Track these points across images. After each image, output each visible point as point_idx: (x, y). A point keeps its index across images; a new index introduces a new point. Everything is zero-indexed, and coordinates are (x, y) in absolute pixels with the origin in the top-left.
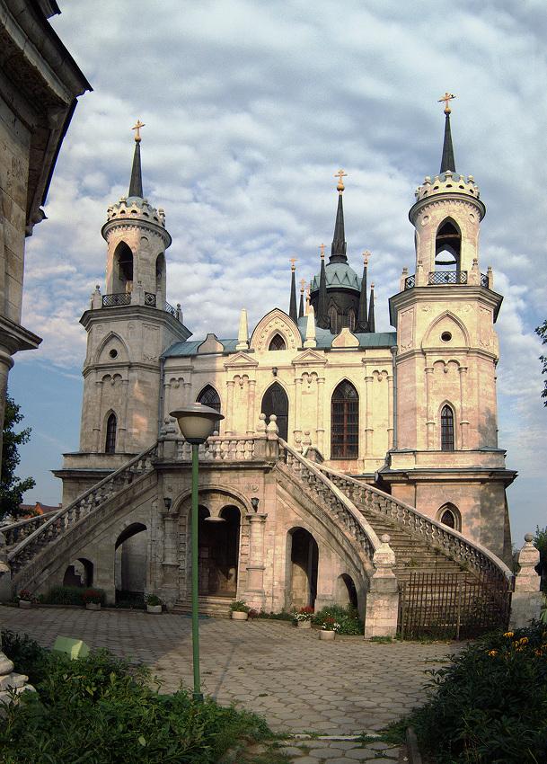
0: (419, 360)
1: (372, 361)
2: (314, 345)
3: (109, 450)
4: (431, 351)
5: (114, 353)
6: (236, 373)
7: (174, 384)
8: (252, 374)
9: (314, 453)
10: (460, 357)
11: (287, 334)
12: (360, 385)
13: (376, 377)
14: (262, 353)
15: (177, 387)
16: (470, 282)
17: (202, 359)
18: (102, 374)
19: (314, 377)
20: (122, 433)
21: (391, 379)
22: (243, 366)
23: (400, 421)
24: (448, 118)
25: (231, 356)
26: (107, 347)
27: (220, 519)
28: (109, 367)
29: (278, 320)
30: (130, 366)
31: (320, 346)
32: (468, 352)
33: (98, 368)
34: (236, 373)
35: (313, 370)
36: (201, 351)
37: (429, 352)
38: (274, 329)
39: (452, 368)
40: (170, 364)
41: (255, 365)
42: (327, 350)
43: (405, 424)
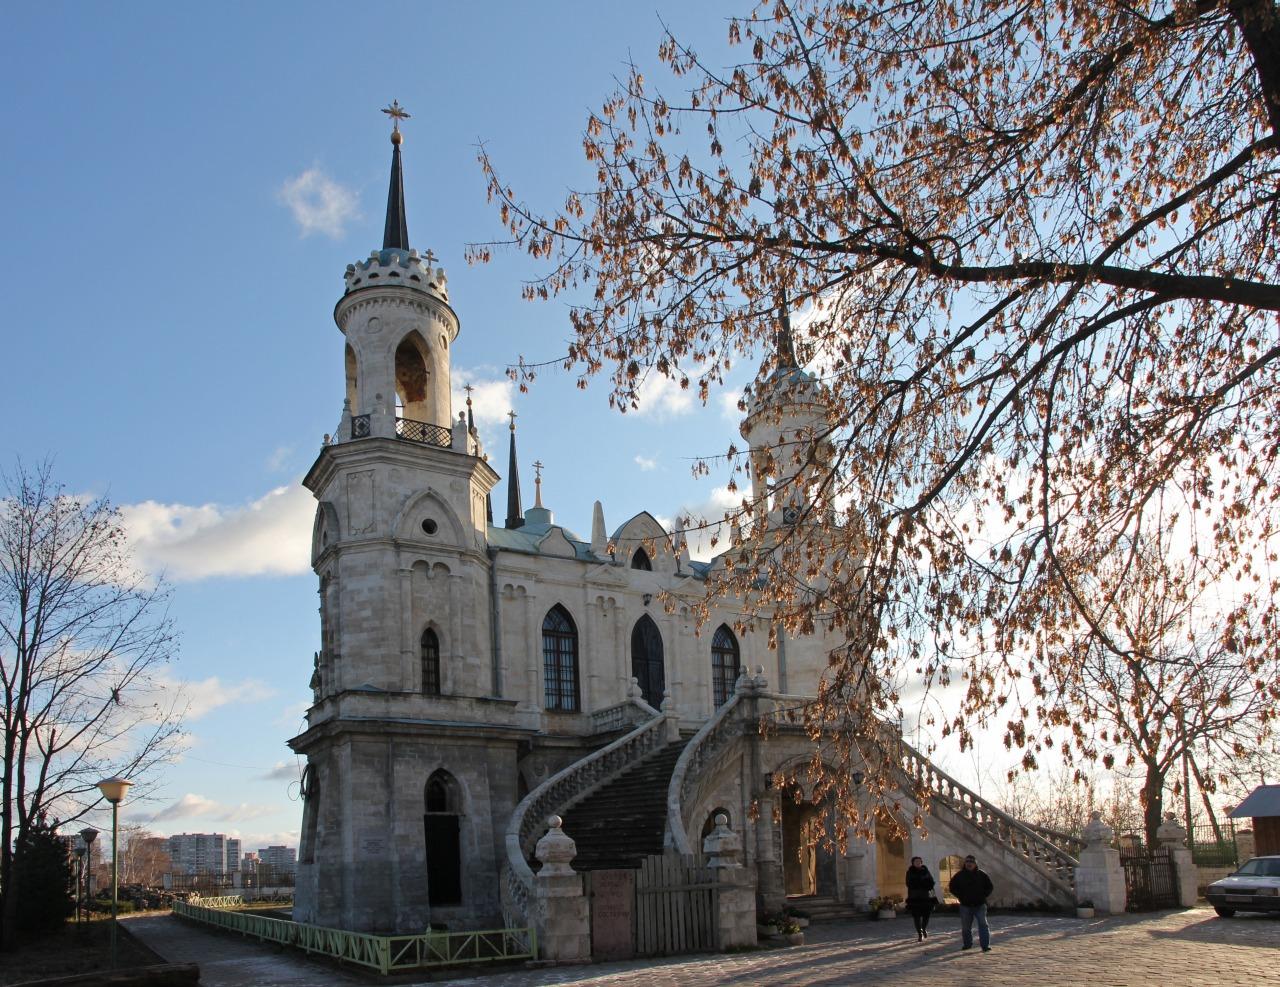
3: (432, 686)
5: (429, 527)
7: (507, 592)
15: (512, 598)
18: (408, 559)
24: (396, 151)
28: (424, 548)
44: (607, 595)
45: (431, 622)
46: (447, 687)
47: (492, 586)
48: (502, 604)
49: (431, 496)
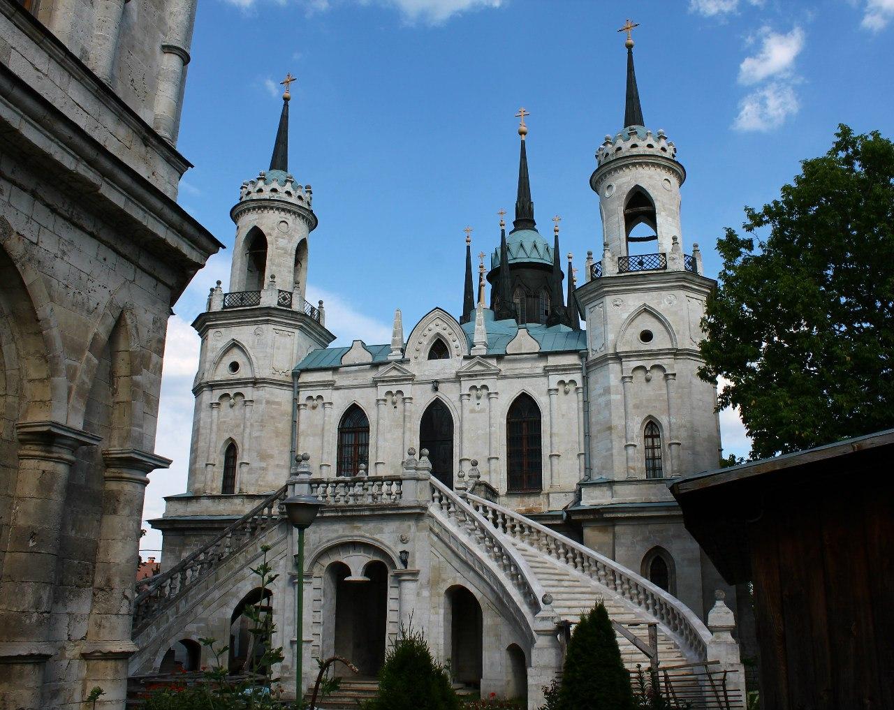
0: (614, 367)
1: (556, 369)
2: (484, 352)
4: (629, 355)
5: (234, 367)
6: (388, 388)
7: (310, 403)
8: (407, 389)
9: (483, 488)
10: (665, 361)
11: (450, 339)
12: (542, 401)
13: (561, 388)
14: (419, 364)
15: (314, 408)
16: (672, 267)
17: (347, 372)
18: (218, 393)
19: (484, 392)
20: (245, 469)
21: (581, 390)
22: (396, 381)
23: (594, 443)
25: (381, 369)
26: (225, 358)
27: (367, 579)
29: (439, 322)
30: (255, 382)
31: (492, 352)
32: (675, 354)
33: (212, 386)
34: (388, 388)
35: (483, 383)
36: (345, 361)
37: (626, 357)
38: (432, 334)
39: (657, 376)
40: (306, 378)
41: (411, 379)
42: (499, 358)
43: (598, 446)
44: (394, 389)
45: (231, 439)
46: (237, 491)
47: (295, 400)
48: (304, 414)
49: (235, 345)
